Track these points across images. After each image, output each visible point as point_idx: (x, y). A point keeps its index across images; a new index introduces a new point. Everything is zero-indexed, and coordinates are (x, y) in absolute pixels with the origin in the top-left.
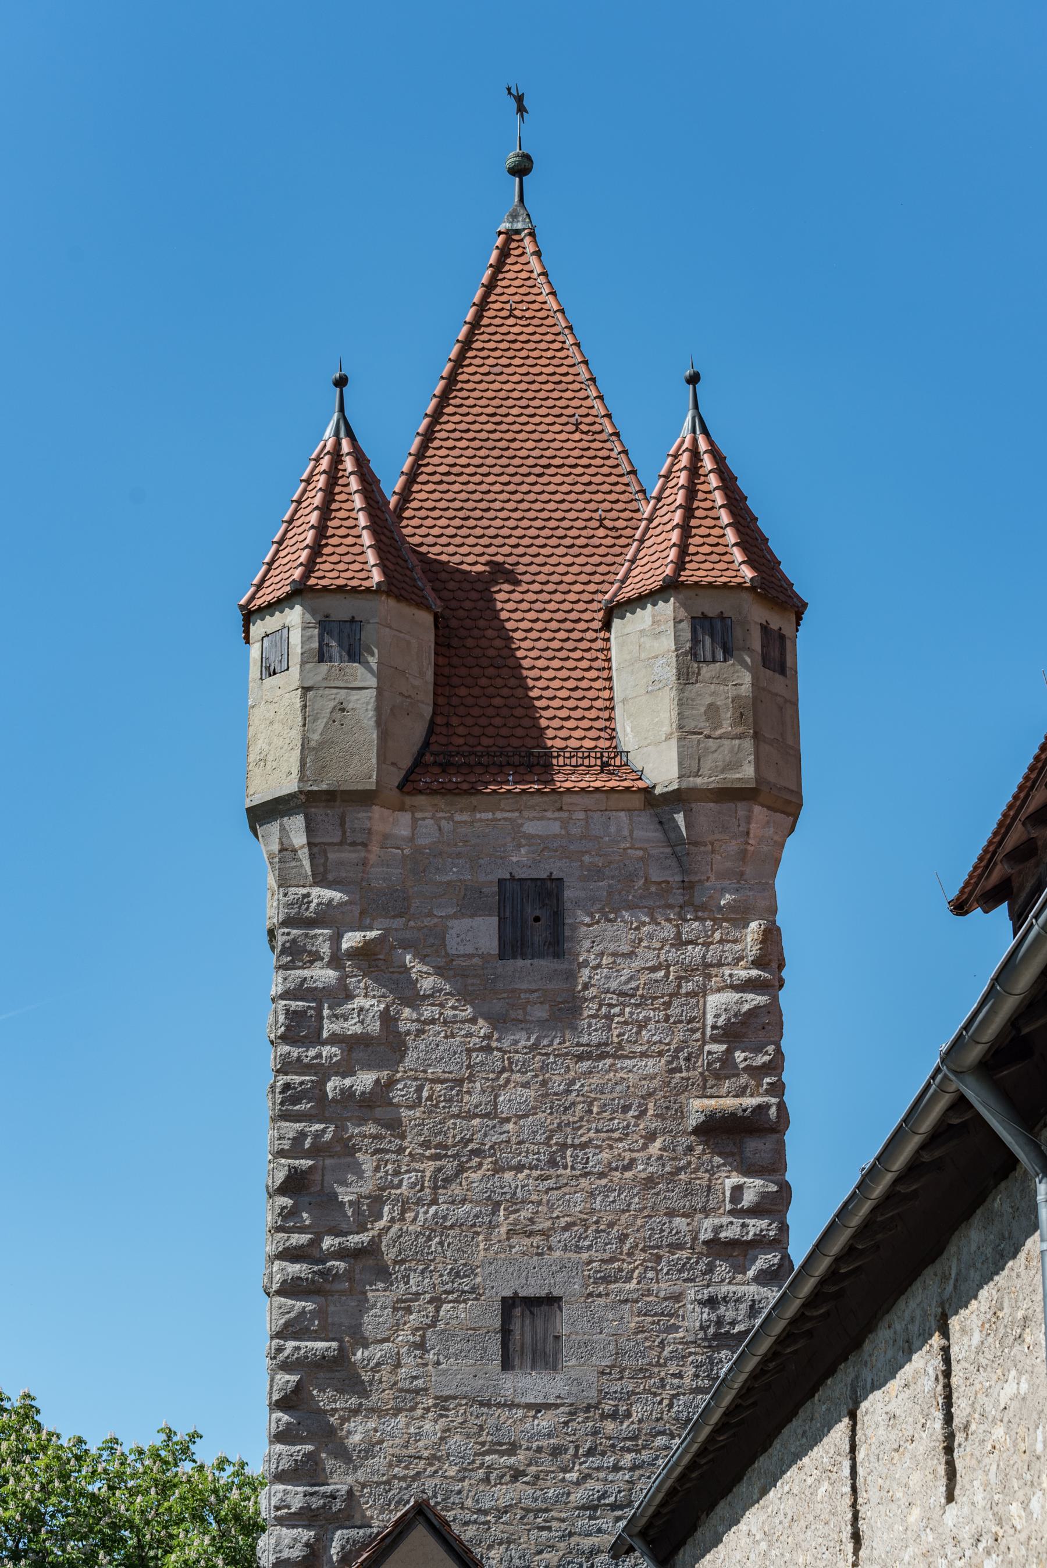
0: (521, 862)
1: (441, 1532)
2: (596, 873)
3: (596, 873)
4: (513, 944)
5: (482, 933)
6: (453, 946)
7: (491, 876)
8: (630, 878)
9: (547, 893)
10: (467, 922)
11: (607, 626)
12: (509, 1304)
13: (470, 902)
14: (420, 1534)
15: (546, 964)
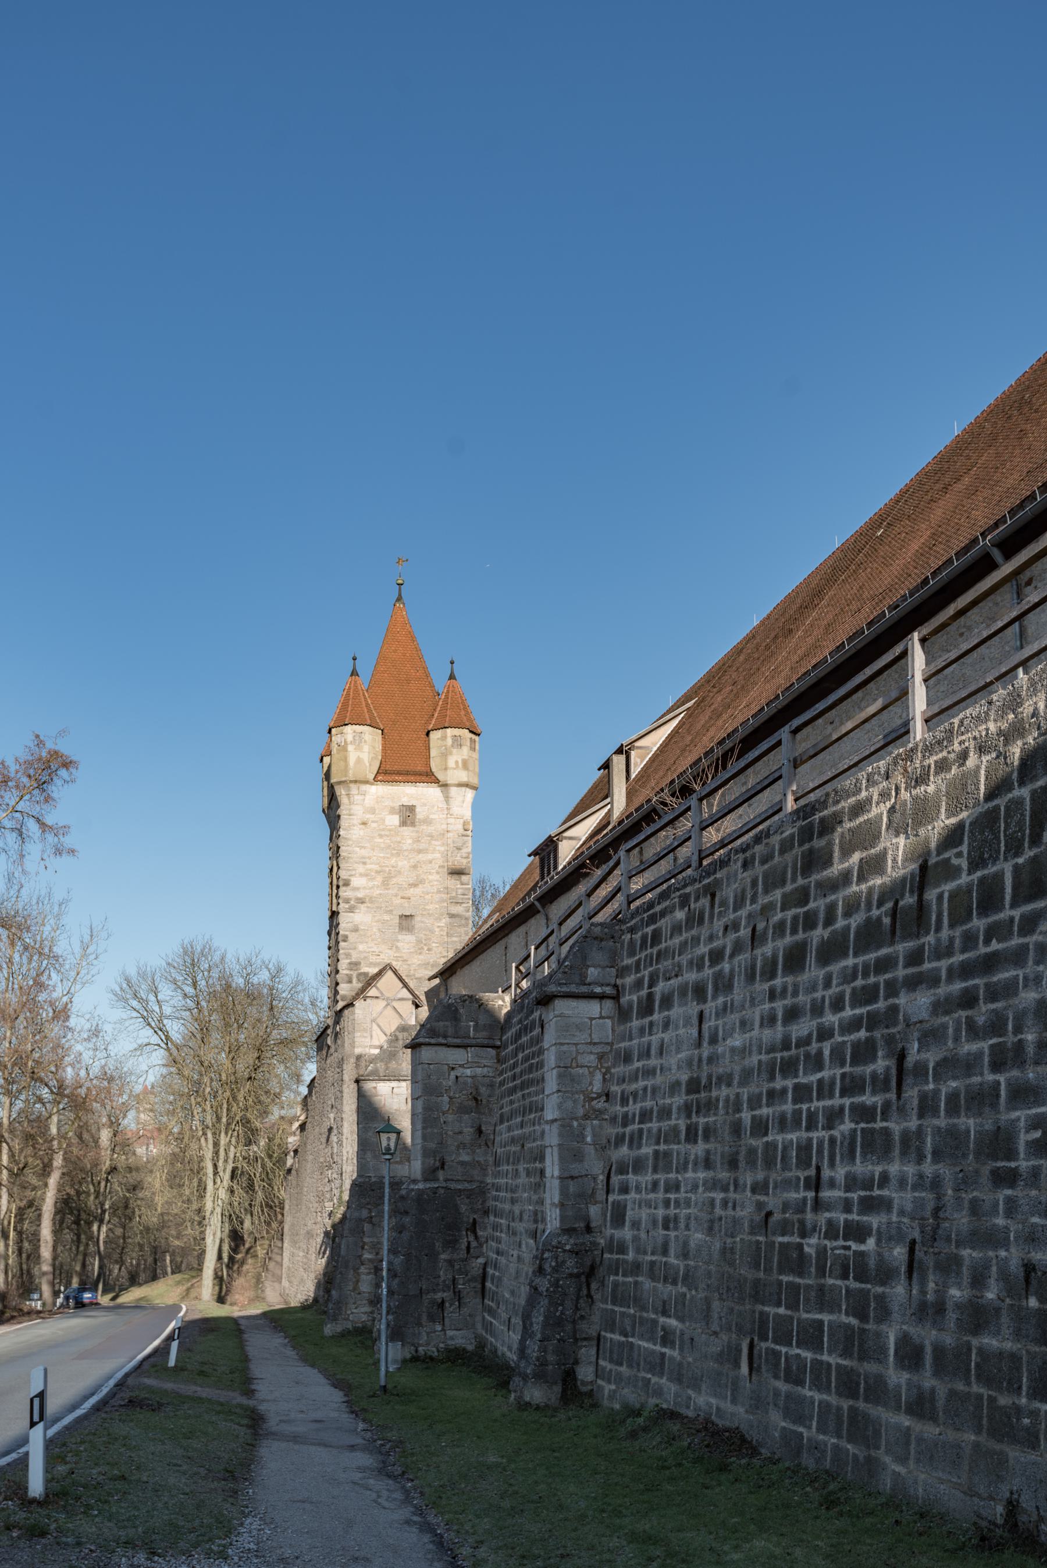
0: (406, 801)
1: (395, 972)
2: (425, 805)
3: (425, 805)
4: (403, 824)
5: (395, 820)
6: (387, 822)
7: (397, 805)
8: (433, 806)
9: (411, 809)
10: (390, 816)
11: (428, 734)
12: (401, 917)
13: (392, 811)
14: (389, 974)
15: (411, 828)
